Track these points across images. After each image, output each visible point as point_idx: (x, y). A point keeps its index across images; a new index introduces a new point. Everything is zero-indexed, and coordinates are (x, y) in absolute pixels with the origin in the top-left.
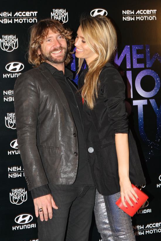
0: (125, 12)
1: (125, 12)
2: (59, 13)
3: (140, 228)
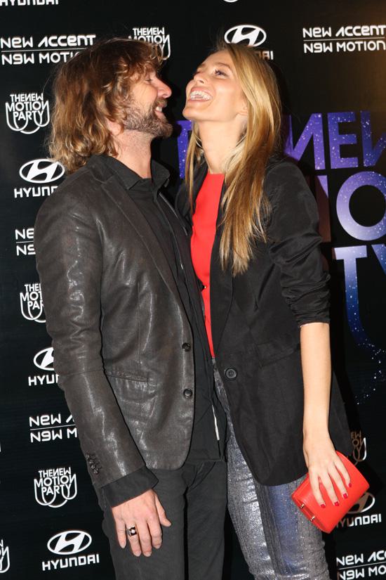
0: (309, 31)
1: (309, 31)
3: (354, 561)
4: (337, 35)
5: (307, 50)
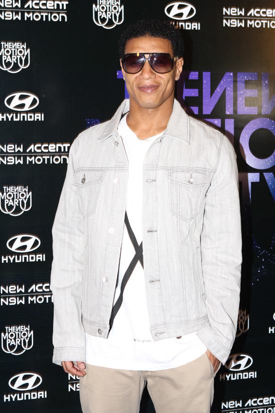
0: (227, 10)
1: (227, 10)
2: (108, 6)
3: (234, 405)
4: (248, 14)
5: (226, 24)
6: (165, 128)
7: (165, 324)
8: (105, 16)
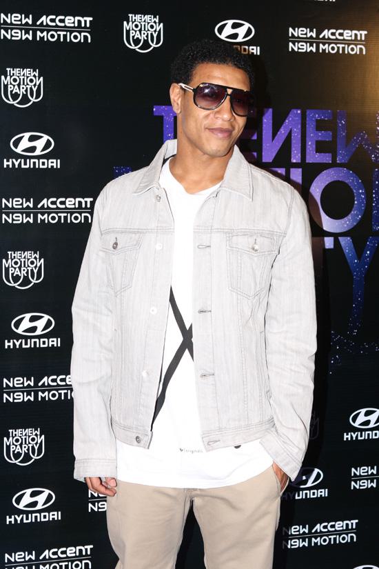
1: (295, 30)
2: (143, 24)
6: (221, 178)
7: (220, 429)
8: (139, 36)
